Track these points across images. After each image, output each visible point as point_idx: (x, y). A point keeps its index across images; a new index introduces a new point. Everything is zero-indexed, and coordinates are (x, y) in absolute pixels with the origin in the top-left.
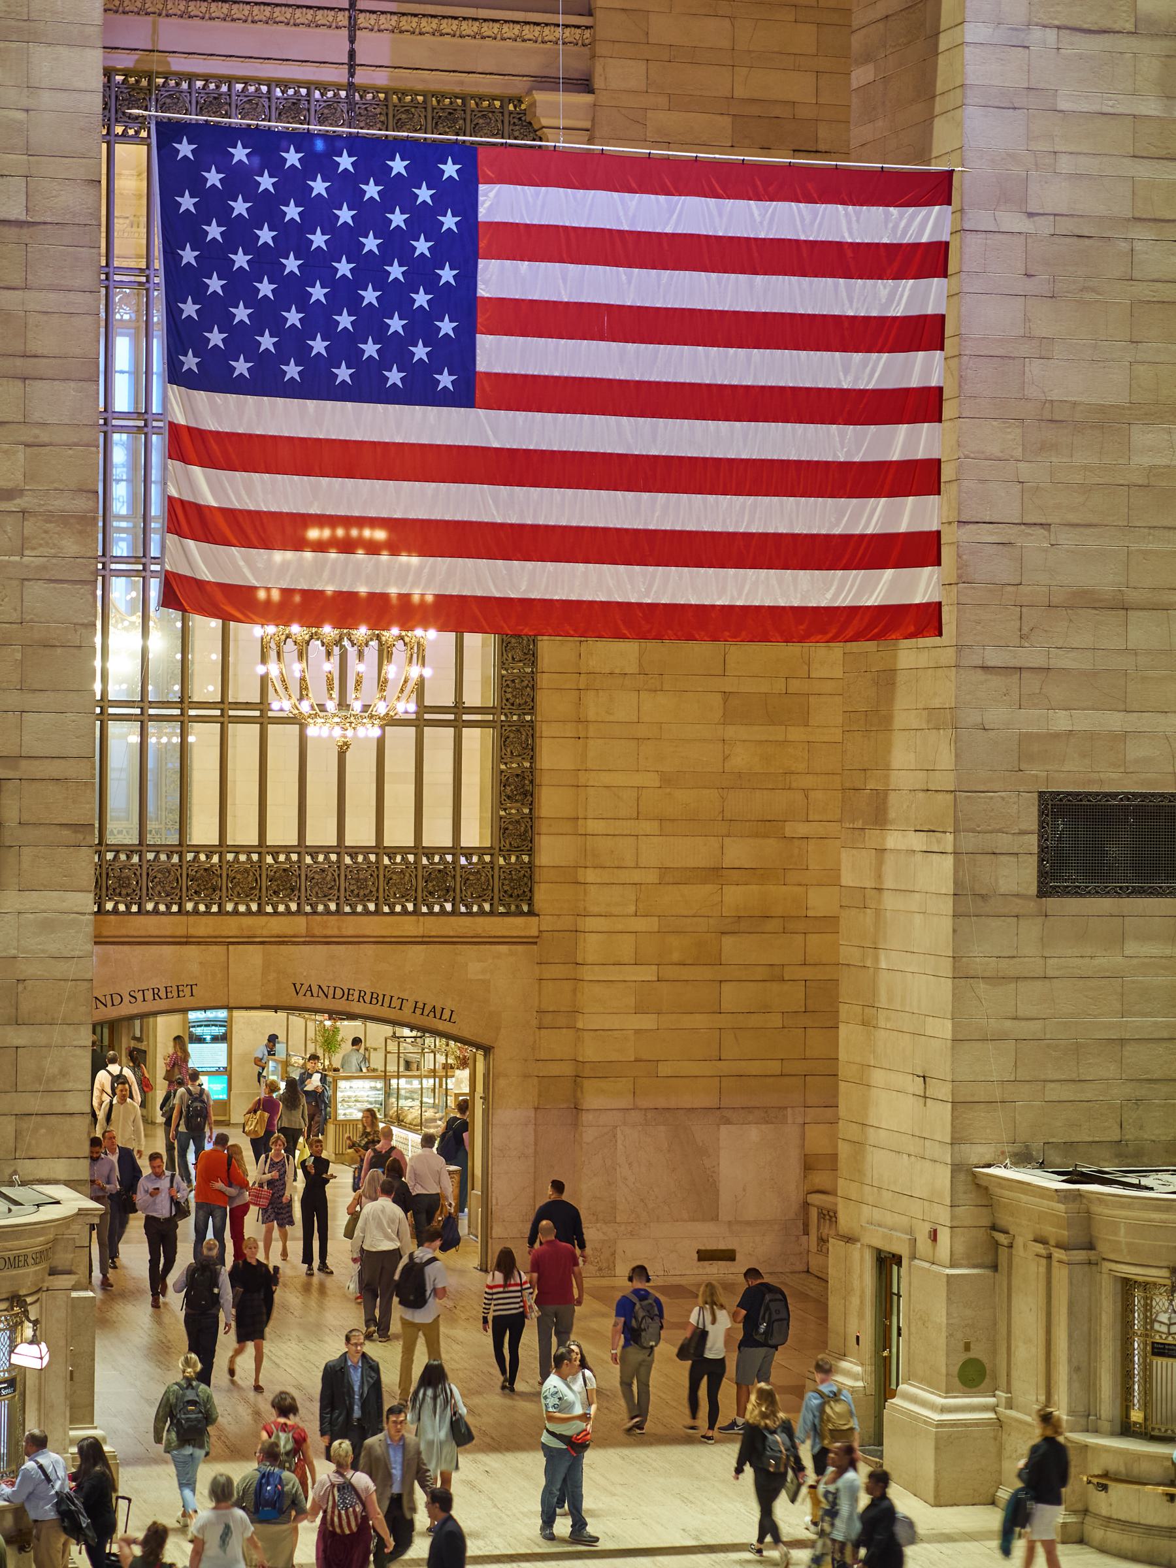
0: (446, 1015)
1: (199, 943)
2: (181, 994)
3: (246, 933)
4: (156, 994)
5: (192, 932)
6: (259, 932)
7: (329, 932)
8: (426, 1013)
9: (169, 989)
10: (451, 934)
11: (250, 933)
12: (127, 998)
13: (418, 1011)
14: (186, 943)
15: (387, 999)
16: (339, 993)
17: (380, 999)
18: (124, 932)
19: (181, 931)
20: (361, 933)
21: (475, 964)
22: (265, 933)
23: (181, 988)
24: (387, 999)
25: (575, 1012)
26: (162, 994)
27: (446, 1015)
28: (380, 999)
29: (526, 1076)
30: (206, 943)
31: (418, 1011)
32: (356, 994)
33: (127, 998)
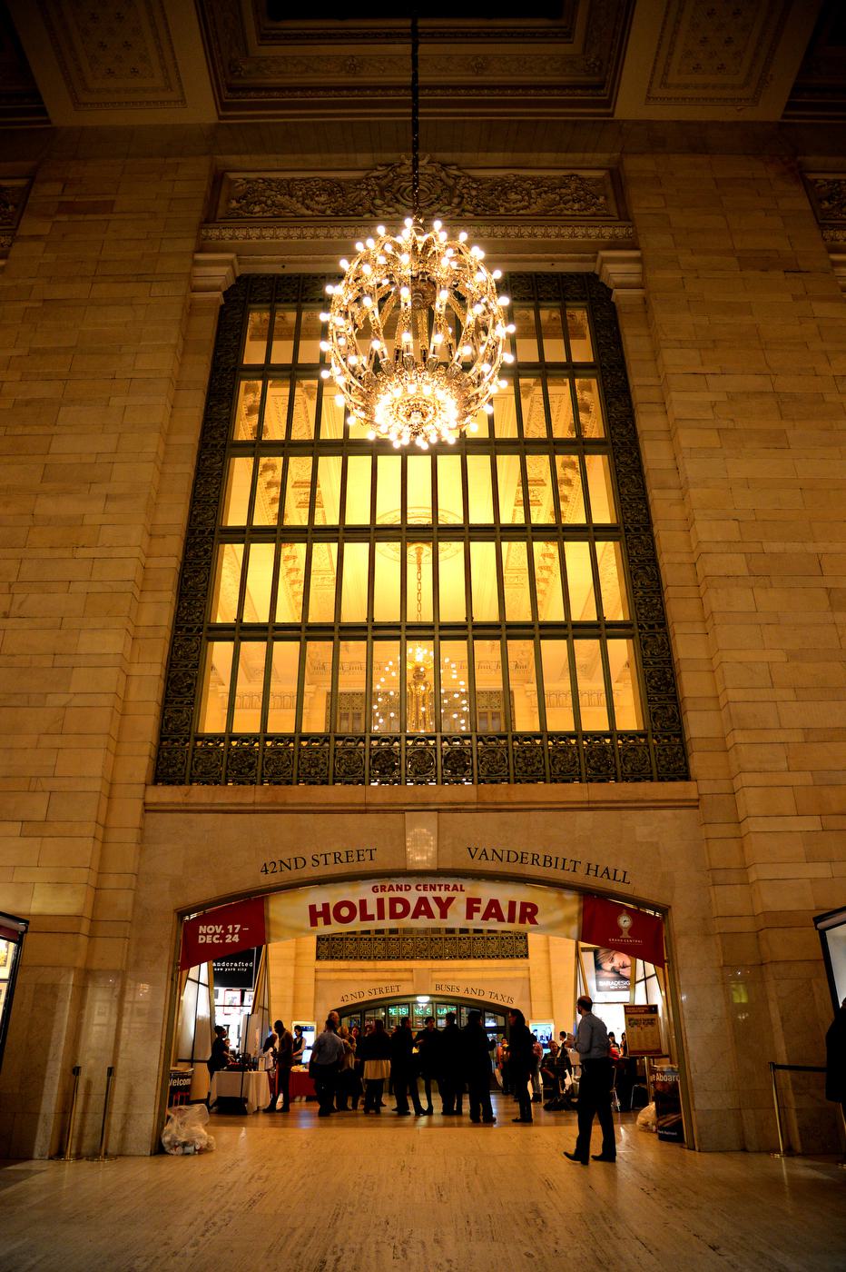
0: (620, 876)
1: (378, 811)
2: (361, 858)
3: (420, 800)
4: (337, 858)
5: (369, 799)
6: (432, 799)
7: (499, 799)
8: (599, 874)
9: (350, 854)
10: (615, 798)
11: (425, 800)
12: (309, 862)
13: (592, 873)
14: (366, 812)
15: (560, 862)
16: (513, 857)
17: (554, 861)
18: (306, 800)
19: (359, 799)
20: (528, 799)
21: (643, 826)
22: (438, 799)
23: (361, 853)
24: (560, 862)
25: (744, 868)
26: (343, 858)
27: (620, 876)
28: (554, 861)
29: (707, 935)
30: (385, 811)
31: (592, 873)
32: (530, 857)
33: (309, 862)
